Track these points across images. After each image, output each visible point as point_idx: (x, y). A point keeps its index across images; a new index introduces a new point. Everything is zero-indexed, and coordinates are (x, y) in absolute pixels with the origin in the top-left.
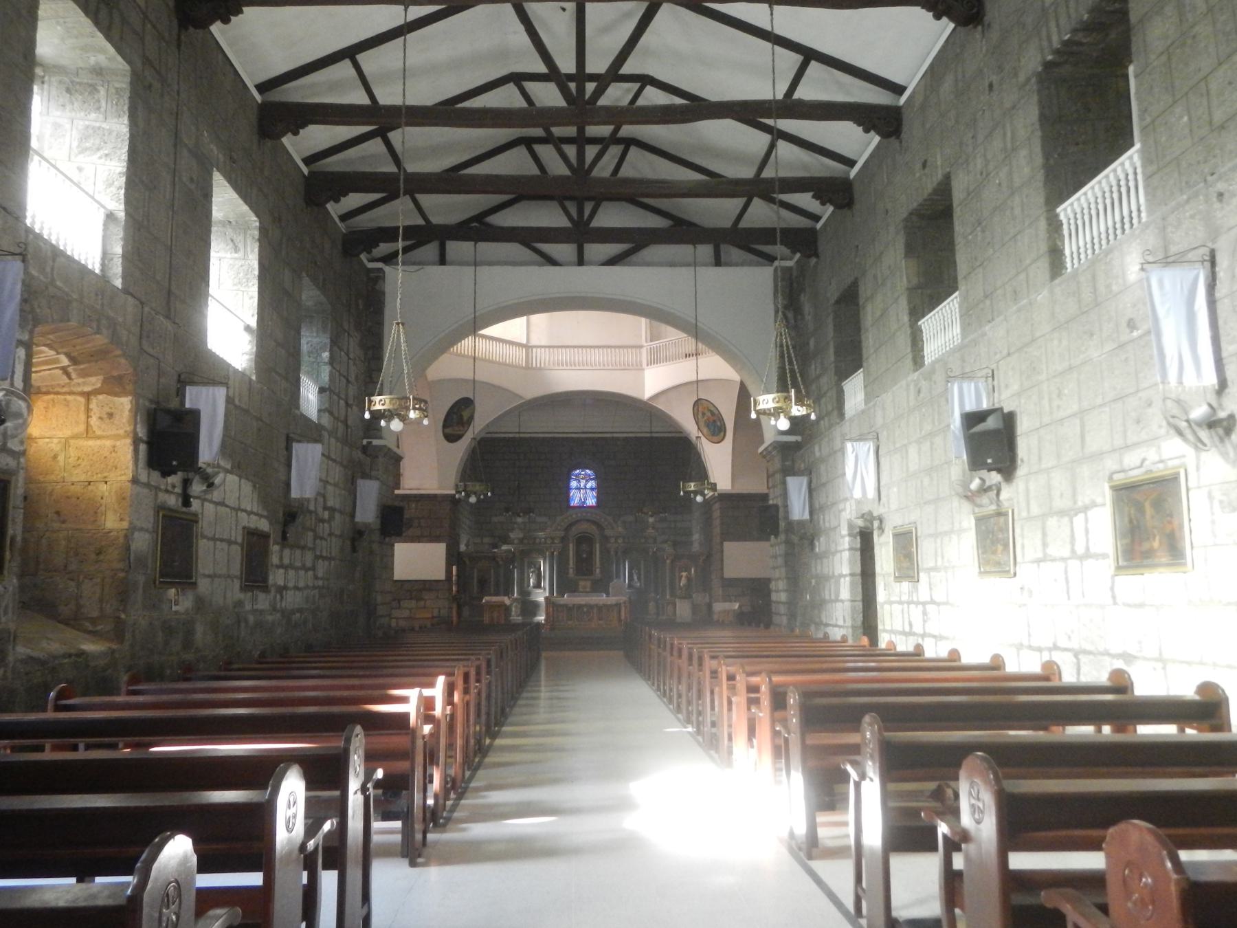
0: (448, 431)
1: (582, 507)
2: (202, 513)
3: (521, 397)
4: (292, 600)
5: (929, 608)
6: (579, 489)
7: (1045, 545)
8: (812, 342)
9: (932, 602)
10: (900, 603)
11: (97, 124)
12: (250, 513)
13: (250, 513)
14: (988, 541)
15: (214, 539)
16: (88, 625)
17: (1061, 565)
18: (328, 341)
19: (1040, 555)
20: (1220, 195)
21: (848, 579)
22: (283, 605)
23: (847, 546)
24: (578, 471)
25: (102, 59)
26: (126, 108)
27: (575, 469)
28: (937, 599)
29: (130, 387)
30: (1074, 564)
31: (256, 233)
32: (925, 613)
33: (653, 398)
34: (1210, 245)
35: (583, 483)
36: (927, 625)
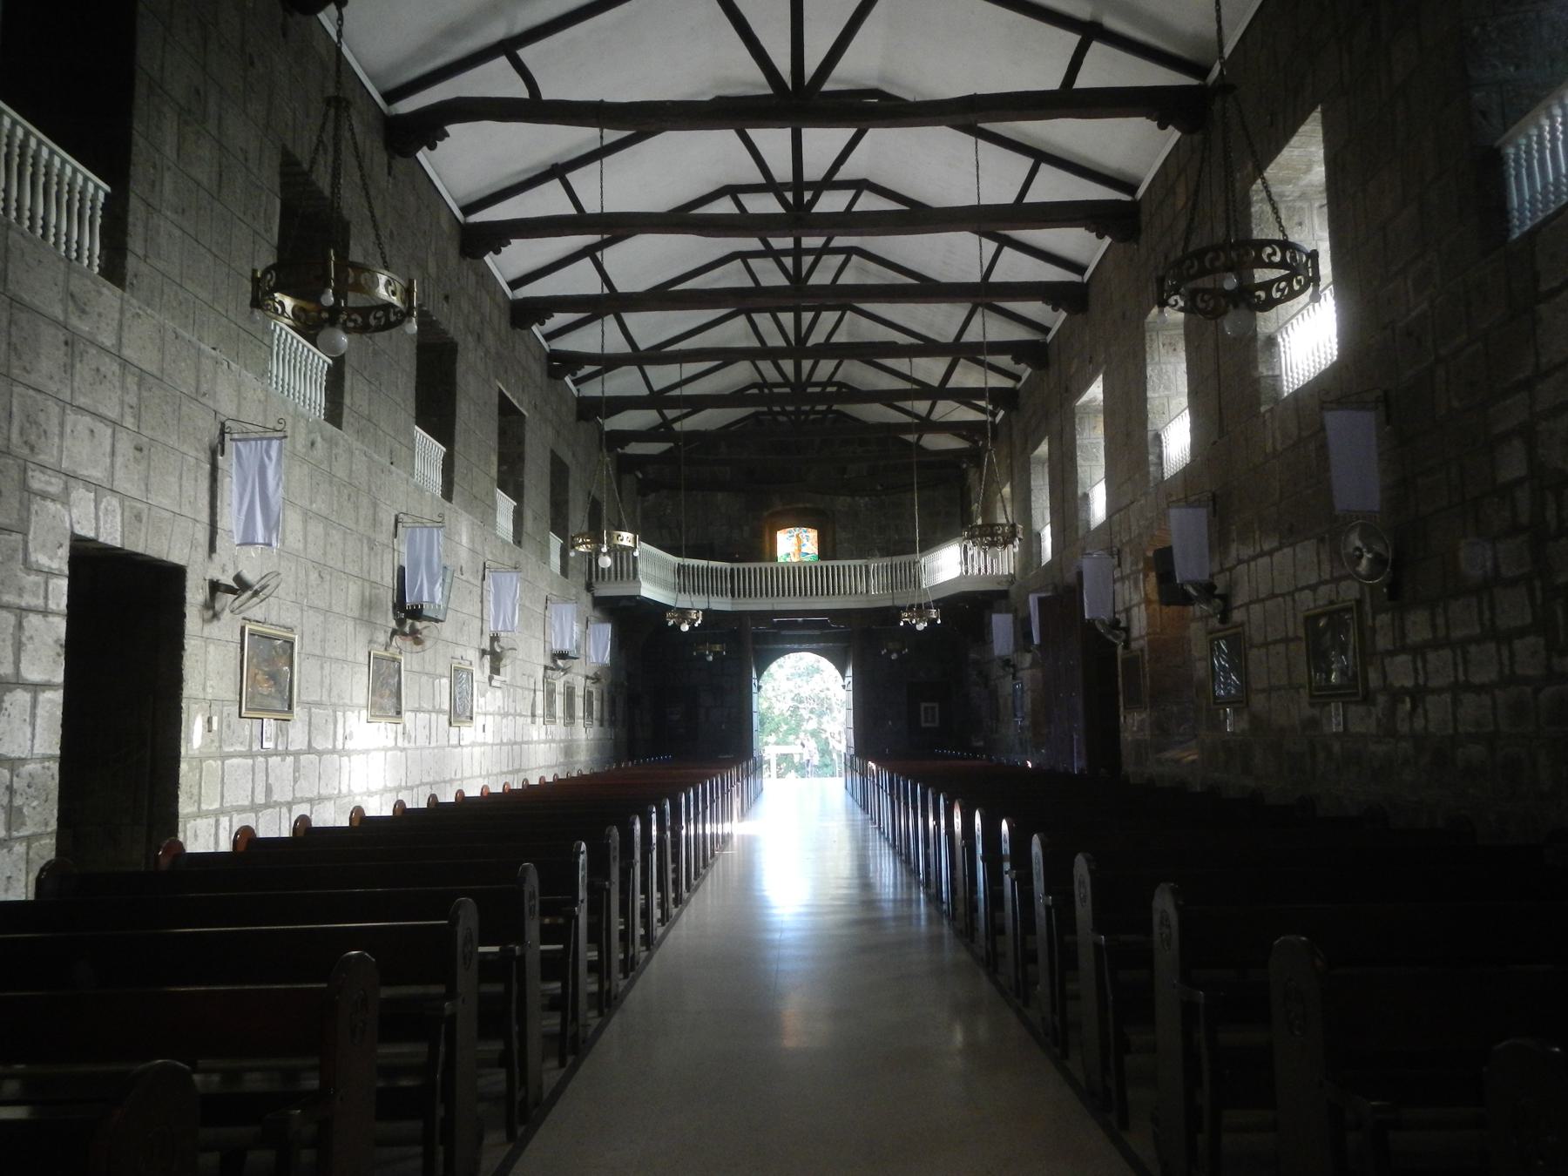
2: (1249, 622)
9: (310, 750)
10: (250, 755)
13: (1313, 588)
14: (379, 684)
15: (1266, 644)
17: (427, 715)
19: (417, 706)
22: (1419, 724)
28: (319, 744)
30: (434, 715)
32: (296, 769)
36: (297, 786)
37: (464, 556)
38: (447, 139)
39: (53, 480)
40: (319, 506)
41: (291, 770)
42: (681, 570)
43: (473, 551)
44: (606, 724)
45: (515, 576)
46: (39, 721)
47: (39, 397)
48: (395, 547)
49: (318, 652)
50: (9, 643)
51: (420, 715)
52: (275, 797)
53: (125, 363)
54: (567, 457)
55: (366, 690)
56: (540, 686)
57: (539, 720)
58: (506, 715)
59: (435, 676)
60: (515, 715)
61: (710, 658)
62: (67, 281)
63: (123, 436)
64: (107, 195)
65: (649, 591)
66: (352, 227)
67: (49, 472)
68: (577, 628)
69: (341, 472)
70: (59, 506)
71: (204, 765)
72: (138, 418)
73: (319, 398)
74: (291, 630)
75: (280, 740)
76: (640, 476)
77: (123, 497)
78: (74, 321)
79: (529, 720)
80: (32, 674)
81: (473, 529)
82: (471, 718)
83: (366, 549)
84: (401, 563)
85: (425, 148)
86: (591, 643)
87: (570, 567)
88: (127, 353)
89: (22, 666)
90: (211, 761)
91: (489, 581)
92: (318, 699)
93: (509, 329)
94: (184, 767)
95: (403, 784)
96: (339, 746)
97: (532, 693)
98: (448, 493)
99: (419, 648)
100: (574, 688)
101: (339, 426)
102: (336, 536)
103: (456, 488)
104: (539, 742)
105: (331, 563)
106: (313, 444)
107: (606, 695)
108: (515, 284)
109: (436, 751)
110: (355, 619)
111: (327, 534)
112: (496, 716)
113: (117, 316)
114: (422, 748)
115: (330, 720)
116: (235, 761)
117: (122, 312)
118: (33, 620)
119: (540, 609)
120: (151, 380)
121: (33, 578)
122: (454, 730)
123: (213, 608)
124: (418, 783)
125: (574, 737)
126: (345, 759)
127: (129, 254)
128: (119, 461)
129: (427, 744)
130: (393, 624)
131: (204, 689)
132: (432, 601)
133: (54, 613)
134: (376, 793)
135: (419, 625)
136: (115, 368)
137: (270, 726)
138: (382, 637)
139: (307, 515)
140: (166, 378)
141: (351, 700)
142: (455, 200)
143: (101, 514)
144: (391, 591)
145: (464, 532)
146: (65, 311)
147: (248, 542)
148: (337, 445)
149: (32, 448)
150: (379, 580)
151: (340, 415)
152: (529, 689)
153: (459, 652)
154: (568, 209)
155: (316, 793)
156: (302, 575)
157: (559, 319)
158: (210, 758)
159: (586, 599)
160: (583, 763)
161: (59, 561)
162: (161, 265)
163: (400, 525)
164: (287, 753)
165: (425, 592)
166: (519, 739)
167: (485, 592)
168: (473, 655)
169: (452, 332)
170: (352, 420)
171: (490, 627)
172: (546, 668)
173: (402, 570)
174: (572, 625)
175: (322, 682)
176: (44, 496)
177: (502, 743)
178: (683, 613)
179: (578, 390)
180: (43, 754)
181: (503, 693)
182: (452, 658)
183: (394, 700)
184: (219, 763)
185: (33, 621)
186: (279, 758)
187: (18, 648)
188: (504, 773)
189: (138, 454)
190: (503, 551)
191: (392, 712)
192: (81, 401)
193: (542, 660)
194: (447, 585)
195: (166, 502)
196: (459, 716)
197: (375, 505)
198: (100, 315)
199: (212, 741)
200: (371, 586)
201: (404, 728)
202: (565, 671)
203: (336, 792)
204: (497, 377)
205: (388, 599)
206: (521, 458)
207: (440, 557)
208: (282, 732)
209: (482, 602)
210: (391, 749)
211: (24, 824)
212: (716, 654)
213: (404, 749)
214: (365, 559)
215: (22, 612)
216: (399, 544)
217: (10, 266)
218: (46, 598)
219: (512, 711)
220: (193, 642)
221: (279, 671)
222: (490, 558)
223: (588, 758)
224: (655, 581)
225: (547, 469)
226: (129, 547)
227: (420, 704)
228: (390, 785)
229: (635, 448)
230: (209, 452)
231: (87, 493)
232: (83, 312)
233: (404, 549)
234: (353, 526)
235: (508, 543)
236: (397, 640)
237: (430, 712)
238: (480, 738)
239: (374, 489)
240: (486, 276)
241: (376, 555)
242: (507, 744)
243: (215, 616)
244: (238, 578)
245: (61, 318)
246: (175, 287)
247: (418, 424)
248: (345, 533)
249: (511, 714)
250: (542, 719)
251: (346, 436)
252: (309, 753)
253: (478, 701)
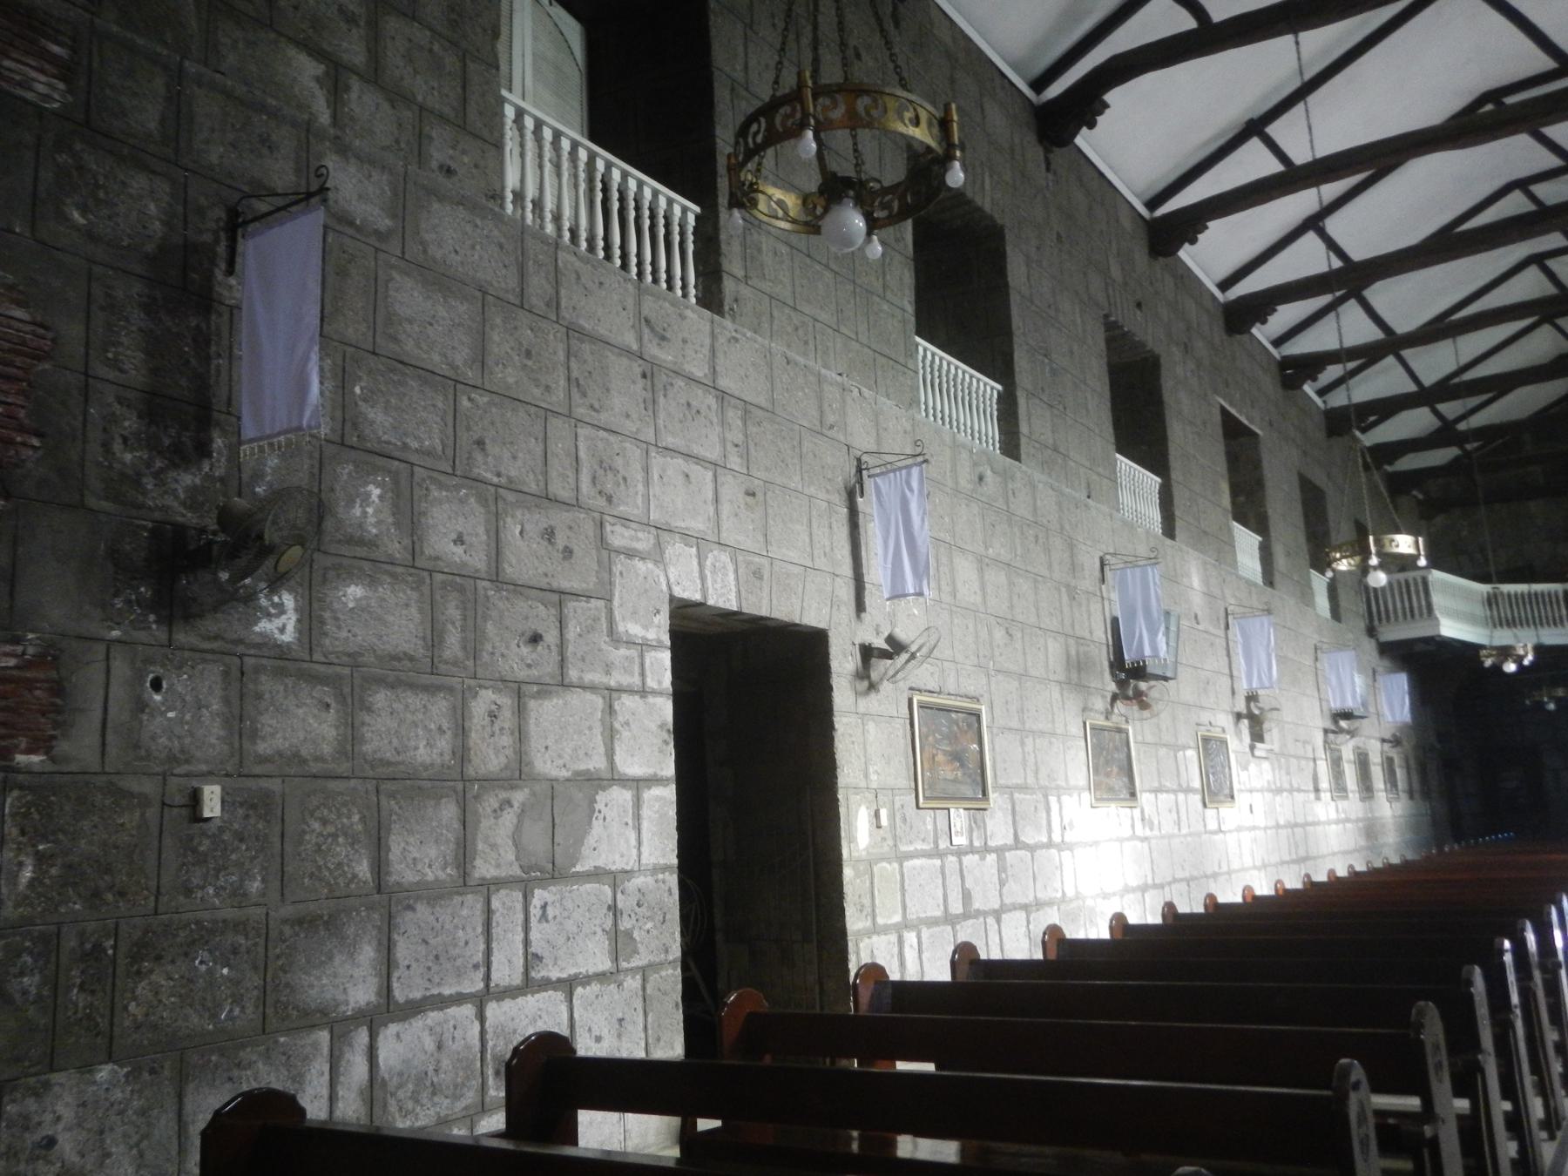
9: (1018, 844)
10: (936, 853)
14: (1102, 759)
17: (1172, 796)
19: (1156, 784)
28: (1029, 837)
30: (1181, 796)
32: (1002, 868)
36: (1005, 890)
37: (1197, 601)
38: (1107, 111)
39: (640, 535)
40: (998, 549)
41: (995, 871)
42: (1491, 601)
43: (1208, 595)
44: (1417, 796)
45: (1265, 620)
46: (645, 825)
47: (612, 438)
48: (1105, 595)
49: (1015, 724)
50: (598, 730)
51: (1163, 797)
52: (977, 904)
53: (722, 395)
54: (1319, 478)
55: (1085, 769)
56: (1321, 753)
57: (1326, 796)
58: (1279, 791)
59: (1177, 748)
60: (1291, 791)
61: (1552, 706)
62: (639, 304)
63: (727, 480)
64: (698, 218)
65: (1451, 629)
66: (1006, 231)
67: (633, 525)
68: (1359, 681)
69: (1021, 508)
70: (650, 565)
71: (875, 869)
72: (747, 458)
73: (993, 431)
74: (977, 700)
75: (975, 834)
76: (1421, 497)
77: (735, 551)
78: (653, 350)
79: (1312, 796)
80: (631, 766)
81: (1206, 570)
82: (1232, 797)
83: (1065, 598)
84: (1115, 614)
85: (1084, 130)
86: (1383, 699)
87: (1342, 611)
88: (723, 383)
89: (617, 759)
90: (885, 864)
91: (1235, 630)
92: (1020, 781)
93: (1225, 337)
94: (848, 872)
95: (1150, 881)
96: (1056, 838)
97: (1312, 764)
98: (1169, 530)
99: (1146, 713)
100: (1366, 755)
101: (1017, 458)
102: (1024, 585)
103: (1179, 524)
104: (1329, 823)
105: (1020, 618)
106: (981, 478)
107: (1412, 762)
108: (1225, 285)
110: (1060, 683)
111: (1011, 584)
113: (708, 341)
114: (1170, 837)
115: (1041, 807)
116: (917, 862)
117: (713, 336)
118: (627, 703)
119: (1309, 661)
120: (760, 413)
121: (623, 651)
122: (1210, 813)
123: (869, 677)
124: (1169, 879)
125: (1377, 815)
126: (1066, 854)
127: (725, 276)
128: (726, 509)
129: (1176, 831)
130: (1112, 687)
131: (866, 776)
132: (1156, 655)
133: (654, 693)
134: (1114, 894)
135: (1143, 685)
136: (711, 401)
137: (959, 817)
138: (1100, 704)
139: (982, 563)
140: (778, 410)
141: (1067, 780)
142: (1137, 196)
143: (708, 573)
144: (1104, 649)
145: (1195, 575)
146: (640, 339)
147: (897, 595)
148: (1013, 478)
149: (609, 499)
150: (1087, 635)
151: (1017, 446)
152: (1307, 759)
153: (1205, 717)
154: (1274, 167)
155: (1031, 898)
156: (984, 634)
157: (1287, 315)
158: (883, 859)
159: (1369, 646)
160: (1393, 848)
161: (658, 630)
162: (766, 286)
163: (1107, 568)
164: (986, 849)
165: (1148, 645)
166: (1300, 820)
167: (1231, 644)
168: (1224, 720)
169: (1150, 345)
170: (1032, 451)
171: (1243, 687)
172: (1326, 731)
173: (1115, 621)
174: (1352, 676)
175: (1024, 762)
176: (631, 554)
177: (1278, 826)
178: (1505, 652)
179: (1325, 402)
180: (655, 865)
181: (1272, 764)
182: (1198, 724)
183: (1126, 779)
184: (896, 865)
185: (627, 703)
186: (977, 857)
187: (610, 735)
188: (1287, 863)
189: (749, 499)
190: (1250, 593)
191: (1125, 794)
192: (669, 441)
193: (1317, 723)
194: (1172, 635)
195: (793, 555)
196: (1216, 794)
197: (1071, 547)
198: (685, 341)
199: (884, 839)
200: (1077, 643)
201: (1142, 812)
202: (1352, 733)
203: (1059, 895)
204: (1216, 392)
205: (1103, 658)
206: (1260, 483)
207: (1158, 600)
208: (976, 824)
209: (1229, 655)
210: (1128, 839)
211: (636, 951)
212: (1558, 701)
213: (1145, 839)
214: (1066, 609)
215: (611, 694)
216: (1108, 591)
217: (563, 292)
218: (643, 674)
219: (1286, 786)
220: (845, 720)
221: (965, 750)
222: (1233, 601)
223: (1398, 840)
224: (1457, 615)
225: (1296, 494)
226: (751, 608)
227: (1160, 782)
228: (1134, 883)
229: (1409, 463)
230: (844, 495)
231: (687, 548)
232: (663, 338)
233: (1115, 596)
234: (1045, 573)
235: (1255, 585)
236: (1120, 706)
237: (1174, 792)
238: (1248, 820)
239: (1067, 527)
240: (1186, 279)
241: (1080, 605)
242: (1285, 827)
243: (872, 687)
244: (891, 639)
245: (635, 347)
246: (787, 310)
247: (1121, 450)
248: (1036, 581)
250: (1329, 794)
251: (1022, 470)
252: (1017, 849)
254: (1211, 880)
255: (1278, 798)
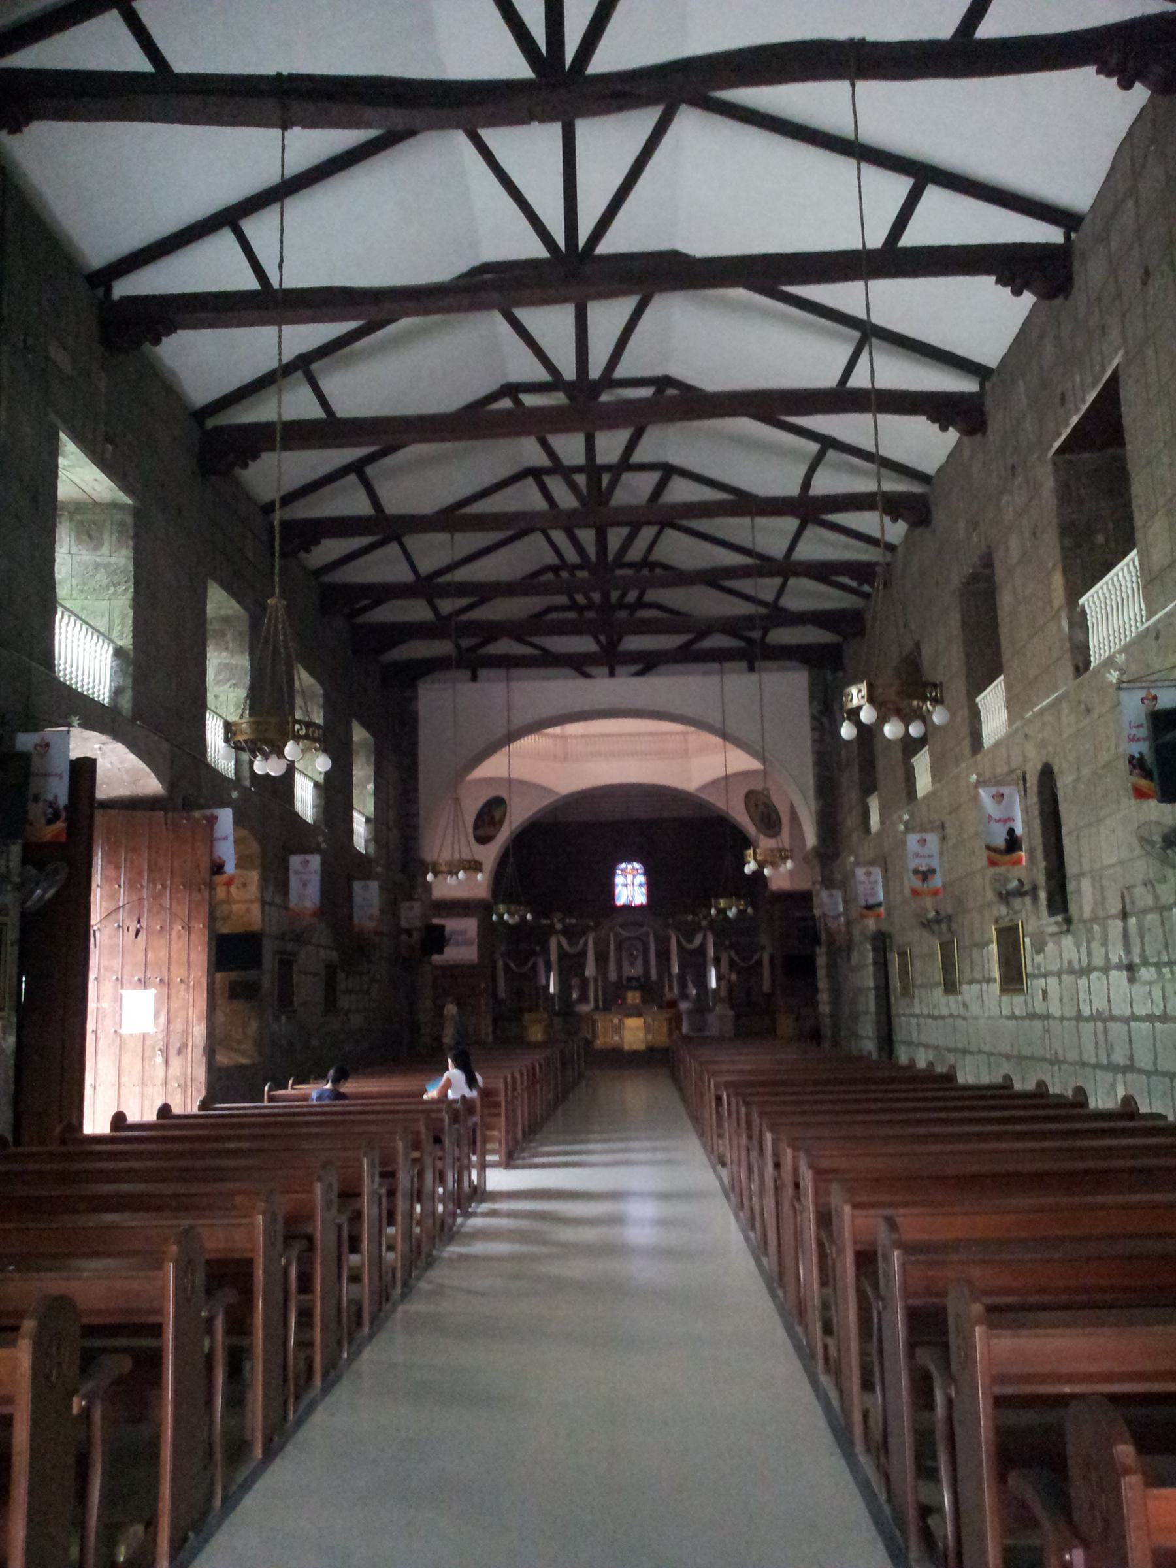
0: (480, 832)
1: (627, 908)
3: (556, 793)
4: (356, 1021)
5: (922, 1020)
6: (626, 885)
7: (972, 970)
8: (843, 752)
11: (227, 661)
12: (325, 948)
16: (235, 1045)
17: (979, 986)
18: (372, 773)
19: (970, 978)
20: (1026, 736)
21: (873, 992)
23: (870, 961)
24: (623, 865)
25: (230, 612)
26: (247, 646)
27: (621, 863)
29: (258, 862)
30: (984, 986)
31: (321, 700)
32: (918, 1025)
33: (698, 789)
34: (1023, 768)
35: (630, 877)
51: (973, 986)
109: (990, 1022)
112: (1064, 977)
114: (976, 1018)
129: (981, 1013)
237: (979, 982)
242: (1092, 1018)
249: (1096, 969)
253: (1033, 960)
254: (1004, 1060)
255: (1083, 982)
